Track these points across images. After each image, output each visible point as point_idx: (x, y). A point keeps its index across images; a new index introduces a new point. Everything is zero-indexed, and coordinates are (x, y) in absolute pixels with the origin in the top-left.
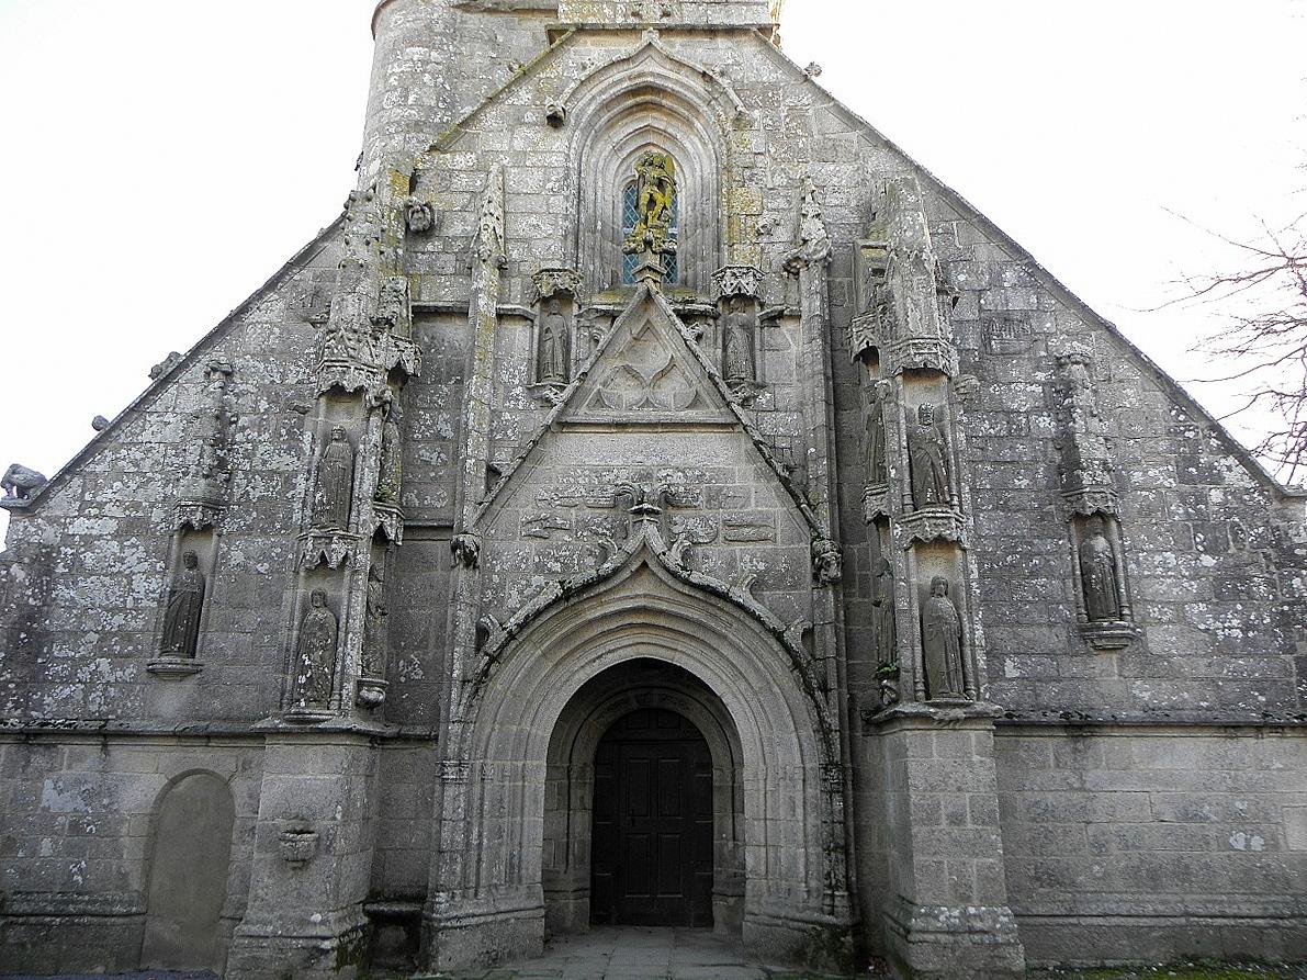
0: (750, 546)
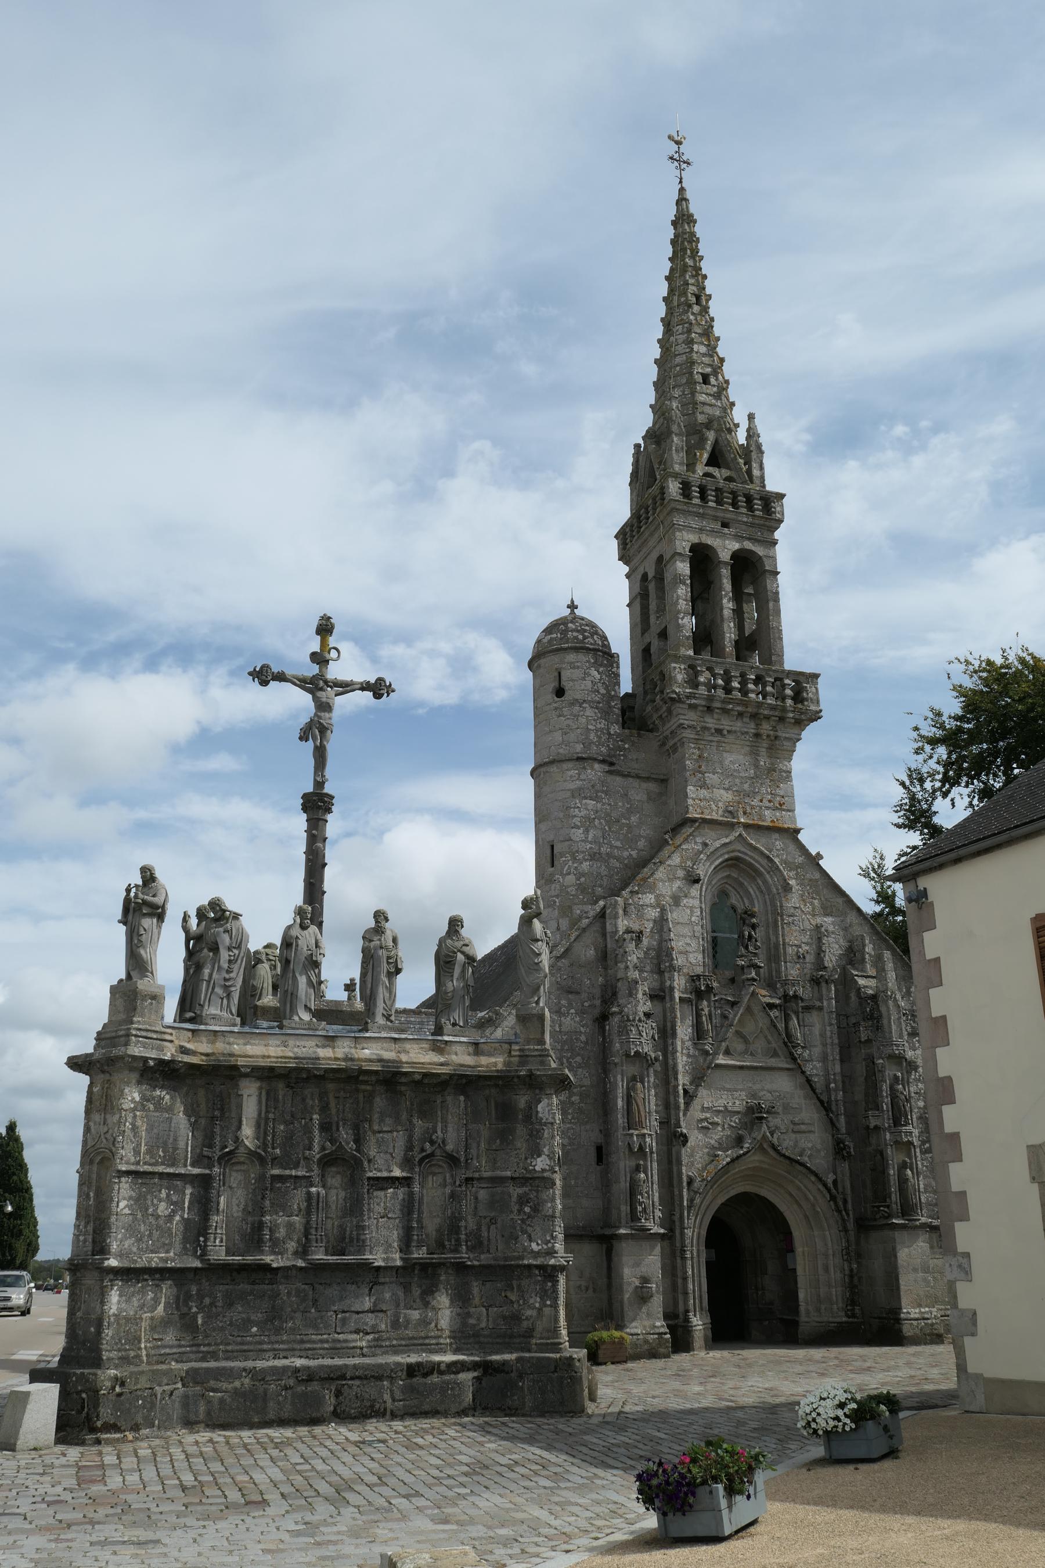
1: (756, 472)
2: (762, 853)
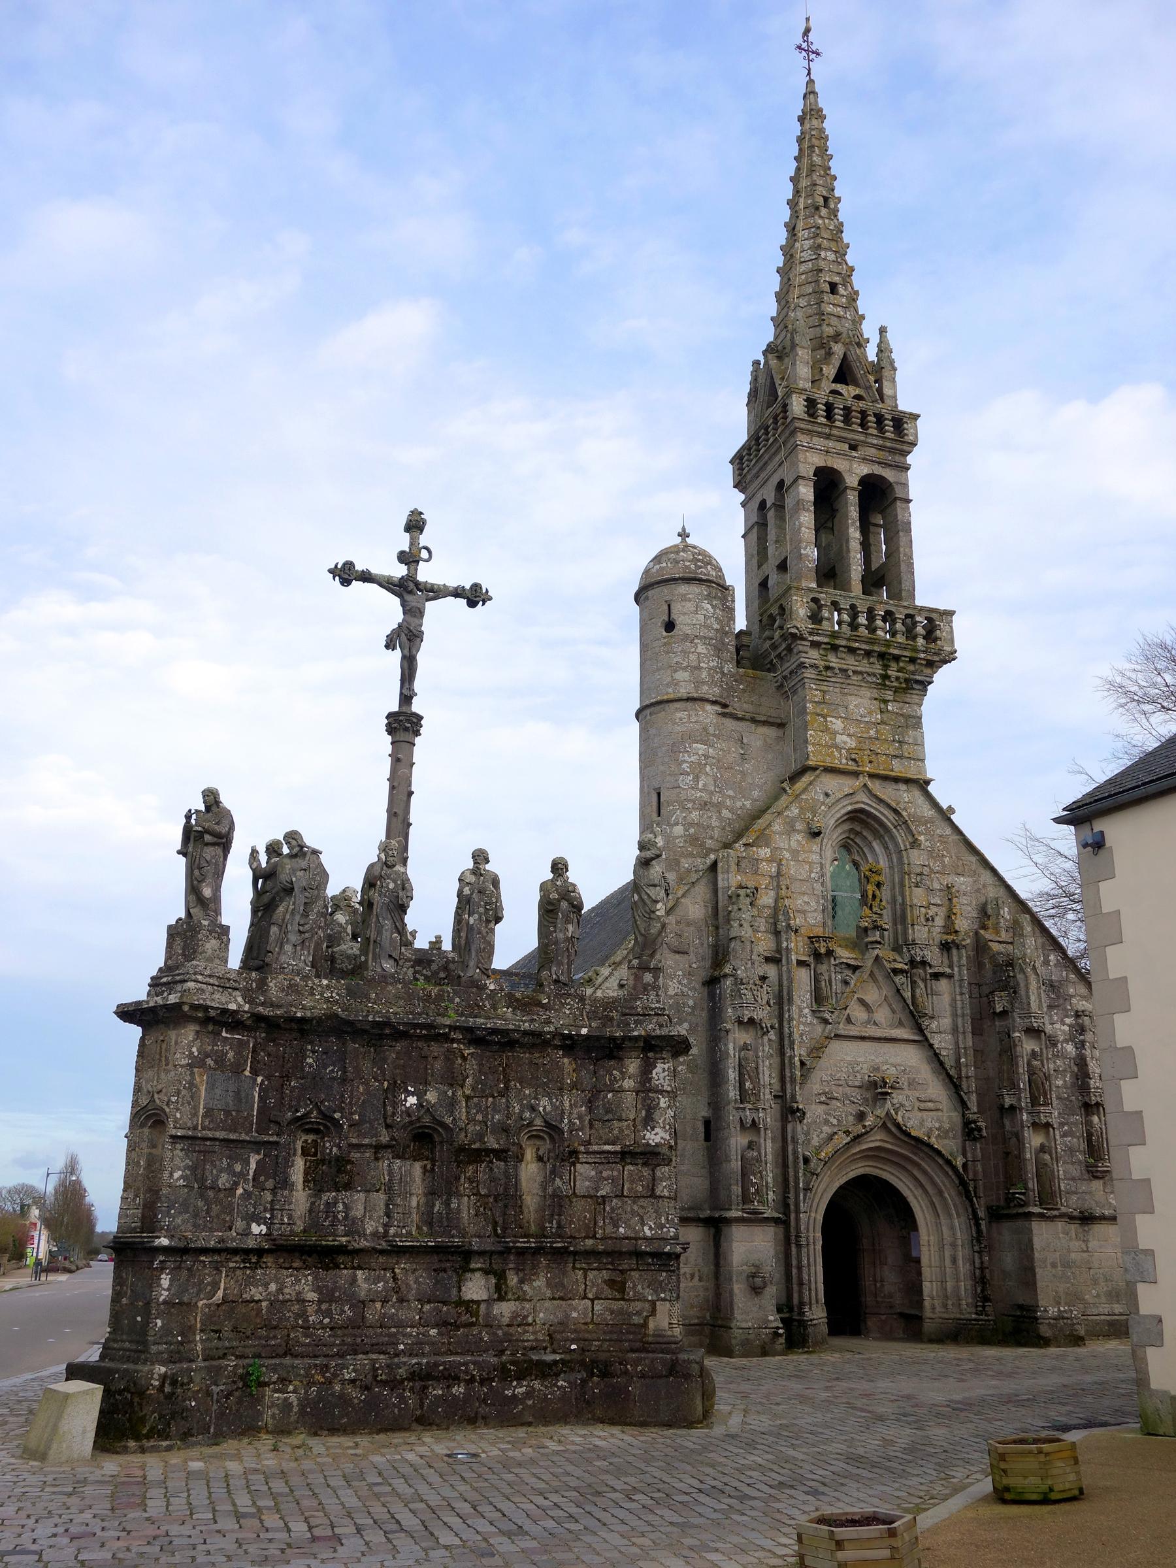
0: (931, 1113)
1: (887, 391)
2: (889, 806)
